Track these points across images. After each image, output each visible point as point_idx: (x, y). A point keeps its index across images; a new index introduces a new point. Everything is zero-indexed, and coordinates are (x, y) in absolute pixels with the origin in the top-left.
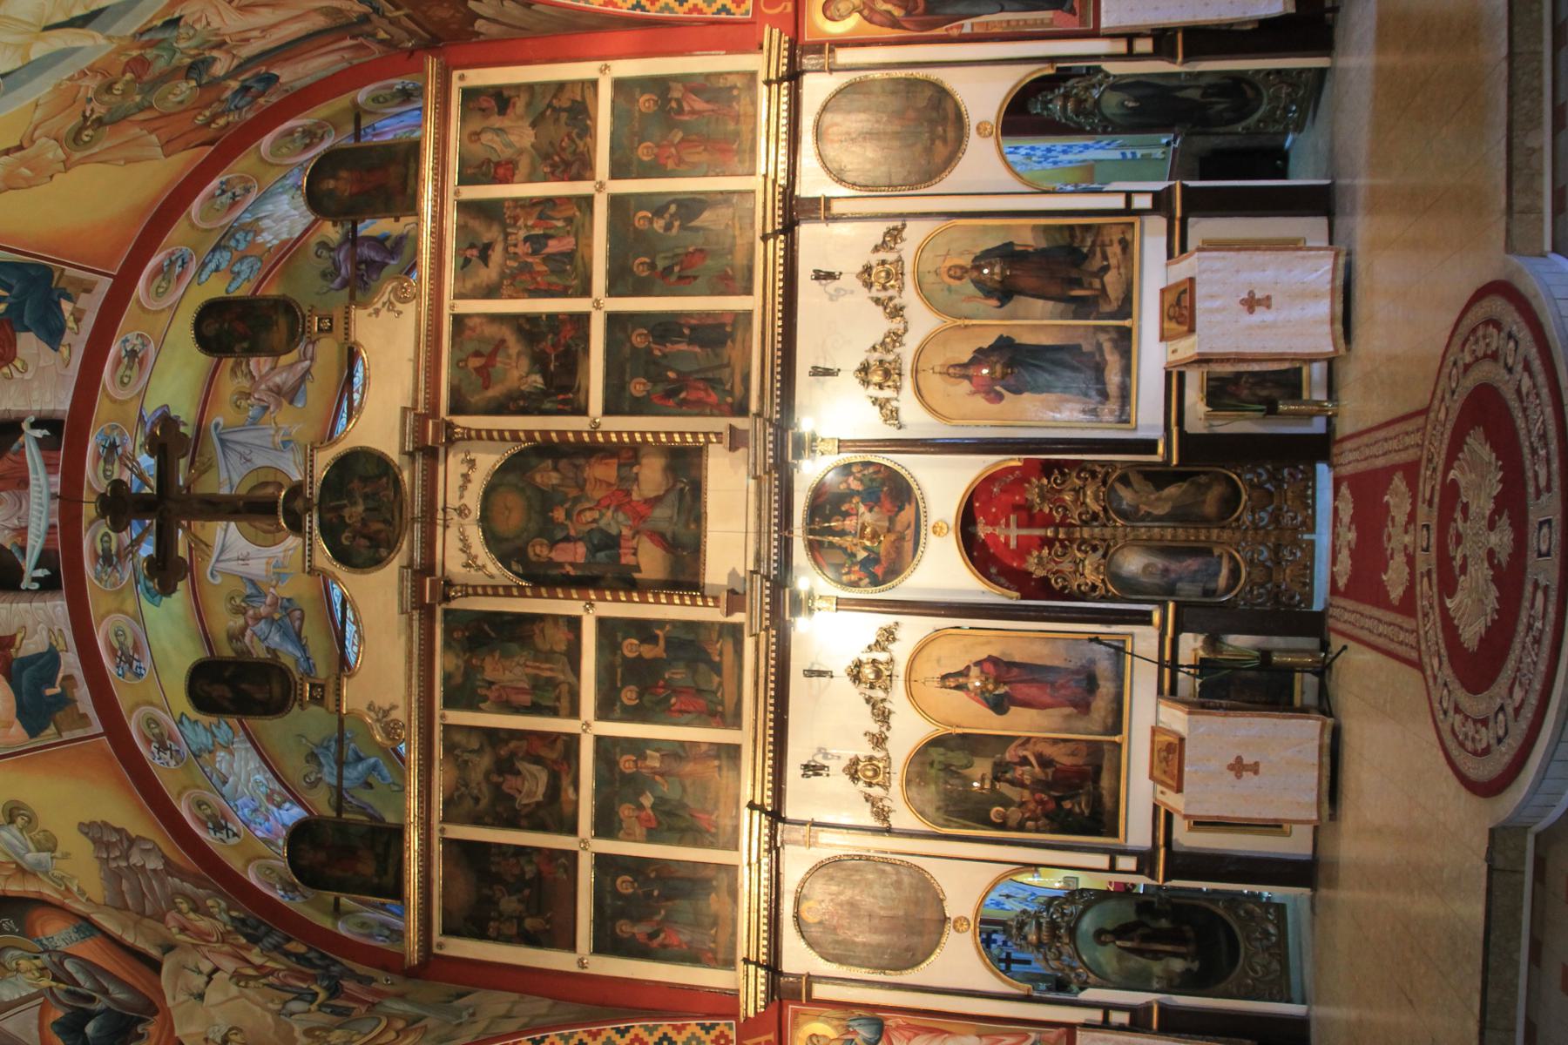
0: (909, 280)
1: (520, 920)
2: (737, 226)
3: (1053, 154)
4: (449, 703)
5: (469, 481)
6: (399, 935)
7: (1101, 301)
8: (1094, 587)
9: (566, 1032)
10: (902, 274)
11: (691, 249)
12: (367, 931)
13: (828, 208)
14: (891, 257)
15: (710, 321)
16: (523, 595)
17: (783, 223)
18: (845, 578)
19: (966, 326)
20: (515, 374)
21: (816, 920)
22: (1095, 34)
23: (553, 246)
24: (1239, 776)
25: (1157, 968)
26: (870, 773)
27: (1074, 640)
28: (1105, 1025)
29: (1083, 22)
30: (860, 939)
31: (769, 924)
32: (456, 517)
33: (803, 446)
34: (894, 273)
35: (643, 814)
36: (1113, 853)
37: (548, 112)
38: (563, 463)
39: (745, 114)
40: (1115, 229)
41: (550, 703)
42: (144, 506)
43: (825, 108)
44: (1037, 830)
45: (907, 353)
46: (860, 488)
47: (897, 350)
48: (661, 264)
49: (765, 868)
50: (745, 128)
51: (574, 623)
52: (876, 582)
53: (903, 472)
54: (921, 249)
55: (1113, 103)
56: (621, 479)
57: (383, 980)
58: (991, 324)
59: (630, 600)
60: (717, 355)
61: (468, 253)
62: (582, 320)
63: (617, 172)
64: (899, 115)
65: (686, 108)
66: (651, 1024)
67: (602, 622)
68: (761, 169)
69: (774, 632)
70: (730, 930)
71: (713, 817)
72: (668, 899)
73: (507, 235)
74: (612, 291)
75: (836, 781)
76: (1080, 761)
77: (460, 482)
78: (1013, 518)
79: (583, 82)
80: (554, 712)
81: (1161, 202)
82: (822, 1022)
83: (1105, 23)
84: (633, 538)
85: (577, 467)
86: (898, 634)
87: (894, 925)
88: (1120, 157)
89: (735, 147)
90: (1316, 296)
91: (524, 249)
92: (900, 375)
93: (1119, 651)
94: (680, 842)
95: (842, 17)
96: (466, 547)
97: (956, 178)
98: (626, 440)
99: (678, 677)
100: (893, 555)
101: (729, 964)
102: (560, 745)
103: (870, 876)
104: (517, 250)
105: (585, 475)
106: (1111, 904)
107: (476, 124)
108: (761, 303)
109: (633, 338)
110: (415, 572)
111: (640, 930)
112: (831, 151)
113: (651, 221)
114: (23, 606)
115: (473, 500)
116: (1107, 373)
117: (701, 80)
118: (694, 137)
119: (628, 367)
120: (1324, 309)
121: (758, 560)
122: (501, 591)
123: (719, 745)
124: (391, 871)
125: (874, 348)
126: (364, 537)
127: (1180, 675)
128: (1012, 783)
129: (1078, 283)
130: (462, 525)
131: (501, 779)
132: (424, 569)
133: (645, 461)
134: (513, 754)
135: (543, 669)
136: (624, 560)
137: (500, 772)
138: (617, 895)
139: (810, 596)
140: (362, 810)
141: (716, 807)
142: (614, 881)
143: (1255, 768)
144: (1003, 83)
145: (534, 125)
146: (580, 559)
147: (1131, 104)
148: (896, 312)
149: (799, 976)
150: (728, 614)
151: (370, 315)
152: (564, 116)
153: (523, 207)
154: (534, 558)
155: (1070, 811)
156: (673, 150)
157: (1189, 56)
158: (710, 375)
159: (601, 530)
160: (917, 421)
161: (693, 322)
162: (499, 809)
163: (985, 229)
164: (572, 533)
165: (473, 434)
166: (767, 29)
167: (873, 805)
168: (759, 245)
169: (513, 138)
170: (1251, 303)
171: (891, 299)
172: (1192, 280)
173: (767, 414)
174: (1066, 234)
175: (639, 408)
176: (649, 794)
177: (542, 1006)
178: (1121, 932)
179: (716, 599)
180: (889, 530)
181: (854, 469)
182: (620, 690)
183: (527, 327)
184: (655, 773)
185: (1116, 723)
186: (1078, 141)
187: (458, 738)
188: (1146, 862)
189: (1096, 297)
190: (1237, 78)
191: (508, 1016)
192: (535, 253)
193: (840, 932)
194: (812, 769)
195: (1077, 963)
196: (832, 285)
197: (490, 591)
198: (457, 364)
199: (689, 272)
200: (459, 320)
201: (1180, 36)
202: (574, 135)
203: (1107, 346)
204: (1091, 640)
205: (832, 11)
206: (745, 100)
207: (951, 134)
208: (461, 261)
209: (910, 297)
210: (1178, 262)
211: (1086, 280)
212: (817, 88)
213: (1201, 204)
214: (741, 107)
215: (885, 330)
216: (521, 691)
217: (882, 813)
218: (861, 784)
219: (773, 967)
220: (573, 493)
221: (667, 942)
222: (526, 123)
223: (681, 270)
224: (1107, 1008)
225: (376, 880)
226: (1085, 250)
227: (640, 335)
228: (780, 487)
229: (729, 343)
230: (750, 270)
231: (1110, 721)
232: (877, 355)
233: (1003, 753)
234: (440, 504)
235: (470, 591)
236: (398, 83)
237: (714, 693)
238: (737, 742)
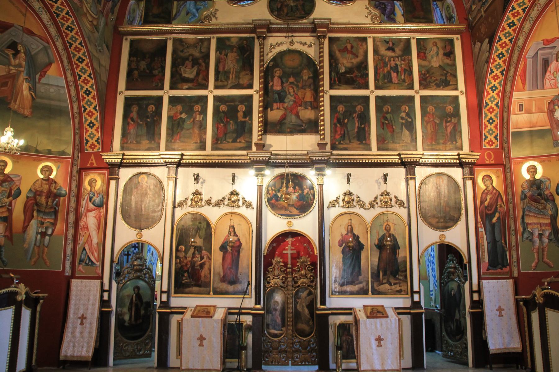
0: (384, 210)
1: (137, 69)
2: (403, 144)
3: (432, 265)
4: (219, 40)
5: (303, 45)
6: (131, 23)
7: (378, 283)
8: (269, 283)
9: (94, 87)
10: (387, 207)
11: (394, 127)
12: (131, 11)
13: (411, 178)
14: (393, 203)
15: (367, 135)
16: (261, 66)
17: (405, 162)
18: (270, 188)
19: (367, 232)
20: (345, 62)
21: (140, 181)
22: (480, 278)
23: (394, 75)
24: (198, 339)
25: (125, 310)
26: (196, 200)
27: (248, 276)
28: (103, 291)
29: (484, 274)
30: (133, 197)
31: (138, 163)
32: (289, 41)
33: (320, 171)
34: (387, 204)
35: (178, 114)
36: (168, 292)
37: (445, 72)
38: (311, 81)
39: (446, 147)
40: (406, 287)
41: (219, 78)
43: (449, 177)
44: (176, 263)
45: (357, 210)
46: (305, 193)
47: (358, 206)
48: (388, 116)
49: (159, 161)
50: (441, 146)
51: (250, 86)
52: (269, 200)
53: (311, 209)
54: (396, 214)
55: (453, 286)
56: (306, 103)
57: (112, 17)
59: (259, 107)
60: (354, 138)
61: (391, 43)
62: (367, 87)
63: (423, 98)
64: (447, 205)
65: (448, 124)
66: (99, 119)
67: (251, 97)
68: (425, 153)
69: (249, 162)
70: (135, 148)
71: (178, 141)
72: (146, 124)
73: (398, 57)
74: (377, 98)
75: (193, 187)
76: (203, 278)
77: (303, 42)
78: (295, 251)
79: (457, 85)
80: (216, 79)
81: (416, 305)
82: (101, 185)
83: (484, 282)
84: (284, 108)
85: (310, 86)
86: (249, 209)
87: (138, 210)
88: (431, 289)
89: (434, 143)
92: (348, 207)
93: (245, 293)
94: (168, 129)
95: (484, 182)
96: (278, 44)
97: (423, 226)
98: (321, 104)
99: (231, 126)
100: (279, 207)
101: (123, 148)
102: (204, 82)
103: (157, 201)
104: (392, 61)
105: (307, 89)
106: (149, 292)
107: (440, 45)
108: (374, 154)
109: (360, 106)
110: (268, 25)
111: (134, 115)
112: (432, 180)
113: (404, 112)
115: (296, 47)
116: (351, 286)
117: (459, 129)
118: (437, 127)
119: (349, 104)
121: (276, 155)
122: (262, 58)
123: (205, 142)
125: (358, 197)
126: (281, 6)
127: (236, 316)
128: (194, 253)
129: (385, 274)
130: (287, 43)
131: (190, 60)
132: (270, 29)
133: (313, 111)
134: (199, 64)
135: (232, 75)
136: (275, 104)
137: (192, 60)
138: (147, 105)
139: (263, 175)
140: (178, 12)
141: (182, 142)
142: (152, 104)
143: (201, 345)
144: (460, 244)
145: (440, 66)
146: (275, 88)
147: (452, 293)
148: (372, 206)
149: (118, 175)
150: (256, 144)
151: (366, 6)
153: (409, 63)
154: (275, 70)
155: (183, 276)
156: (432, 119)
157: (472, 314)
158: (346, 135)
159: (286, 95)
160: (331, 214)
161: (366, 129)
162: (179, 60)
163: (405, 238)
164: (285, 85)
165: (322, 46)
166: (479, 154)
167: (184, 201)
168: (396, 153)
169: (435, 59)
170: (379, 340)
171: (377, 203)
172: (387, 317)
173: (332, 157)
174: (404, 269)
175: (333, 109)
176: (186, 116)
177: (104, 77)
178: (139, 296)
179: (261, 139)
180: (289, 205)
181: (312, 191)
182: (225, 104)
183: (363, 66)
184: (194, 119)
185: (218, 292)
186: (437, 274)
187: (206, 44)
188: (165, 305)
189: (380, 281)
190: (464, 332)
191: (100, 65)
192: (391, 68)
193: (136, 190)
194: (197, 178)
195: (126, 279)
196: (382, 181)
197: (262, 54)
198: (348, 40)
199: (385, 127)
200: (365, 40)
201: (480, 310)
202: (436, 82)
203: (361, 286)
204: (249, 282)
205: (486, 178)
206: (451, 146)
207: (440, 225)
208: (387, 40)
209: (378, 210)
210: (393, 311)
211: (386, 277)
212: (457, 173)
213: (416, 320)
214: (449, 145)
215: (365, 201)
216: (224, 67)
217: (181, 205)
218: (192, 196)
219: (121, 165)
220: (300, 85)
221: (130, 125)
222: (441, 63)
223: (386, 123)
224: (109, 291)
225: (150, 14)
226: (397, 276)
227: (361, 108)
228: (304, 163)
229: (359, 142)
230: (387, 150)
231: (218, 290)
232: (355, 198)
233: (205, 250)
234: (294, 34)
235: (262, 46)
236: (455, 15)
237: (225, 140)
238: (207, 149)
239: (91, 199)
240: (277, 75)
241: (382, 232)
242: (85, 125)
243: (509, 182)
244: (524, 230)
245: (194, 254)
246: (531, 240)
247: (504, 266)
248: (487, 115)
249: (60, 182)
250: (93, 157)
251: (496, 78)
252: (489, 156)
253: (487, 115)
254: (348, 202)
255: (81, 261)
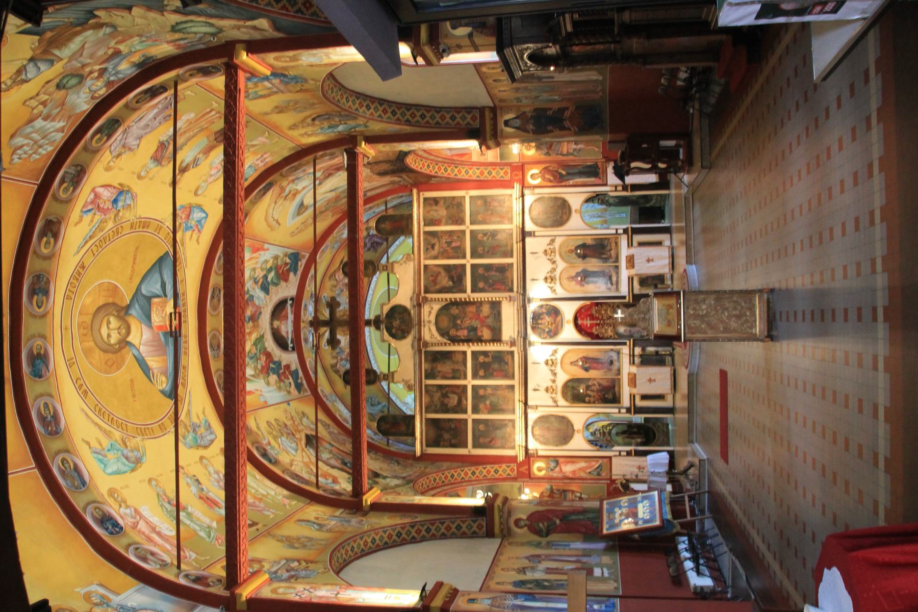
1: (450, 441)
4: (427, 377)
22: (606, 185)
25: (633, 441)
27: (606, 351)
29: (603, 181)
33: (529, 301)
34: (553, 251)
36: (620, 408)
38: (460, 307)
42: (325, 323)
45: (557, 273)
48: (486, 250)
51: (465, 353)
52: (551, 337)
56: (477, 311)
58: (580, 265)
62: (464, 266)
63: (471, 224)
67: (473, 353)
74: (472, 257)
80: (459, 378)
81: (625, 231)
90: (665, 258)
91: (445, 245)
93: (618, 353)
101: (513, 448)
102: (461, 388)
106: (620, 427)
107: (428, 208)
114: (290, 355)
115: (433, 318)
120: (667, 261)
124: (411, 428)
129: (604, 254)
134: (447, 392)
138: (479, 430)
145: (446, 209)
148: (554, 262)
152: (455, 207)
160: (561, 293)
163: (578, 239)
170: (649, 261)
172: (633, 256)
175: (482, 290)
178: (623, 433)
179: (507, 344)
185: (619, 372)
187: (430, 388)
188: (628, 410)
196: (536, 255)
198: (425, 279)
200: (426, 267)
209: (558, 258)
212: (529, 198)
213: (636, 231)
216: (449, 373)
217: (555, 402)
220: (463, 315)
224: (620, 452)
230: (512, 251)
239: (552, 470)
240: (455, 333)
241: (574, 255)
242: (497, 476)
243: (537, 163)
244: (572, 154)
245: (593, 391)
246: (580, 150)
247: (598, 166)
248: (486, 177)
249: (541, 489)
250: (521, 469)
251: (460, 172)
252: (516, 175)
253: (486, 176)
254: (552, 280)
255: (599, 474)
